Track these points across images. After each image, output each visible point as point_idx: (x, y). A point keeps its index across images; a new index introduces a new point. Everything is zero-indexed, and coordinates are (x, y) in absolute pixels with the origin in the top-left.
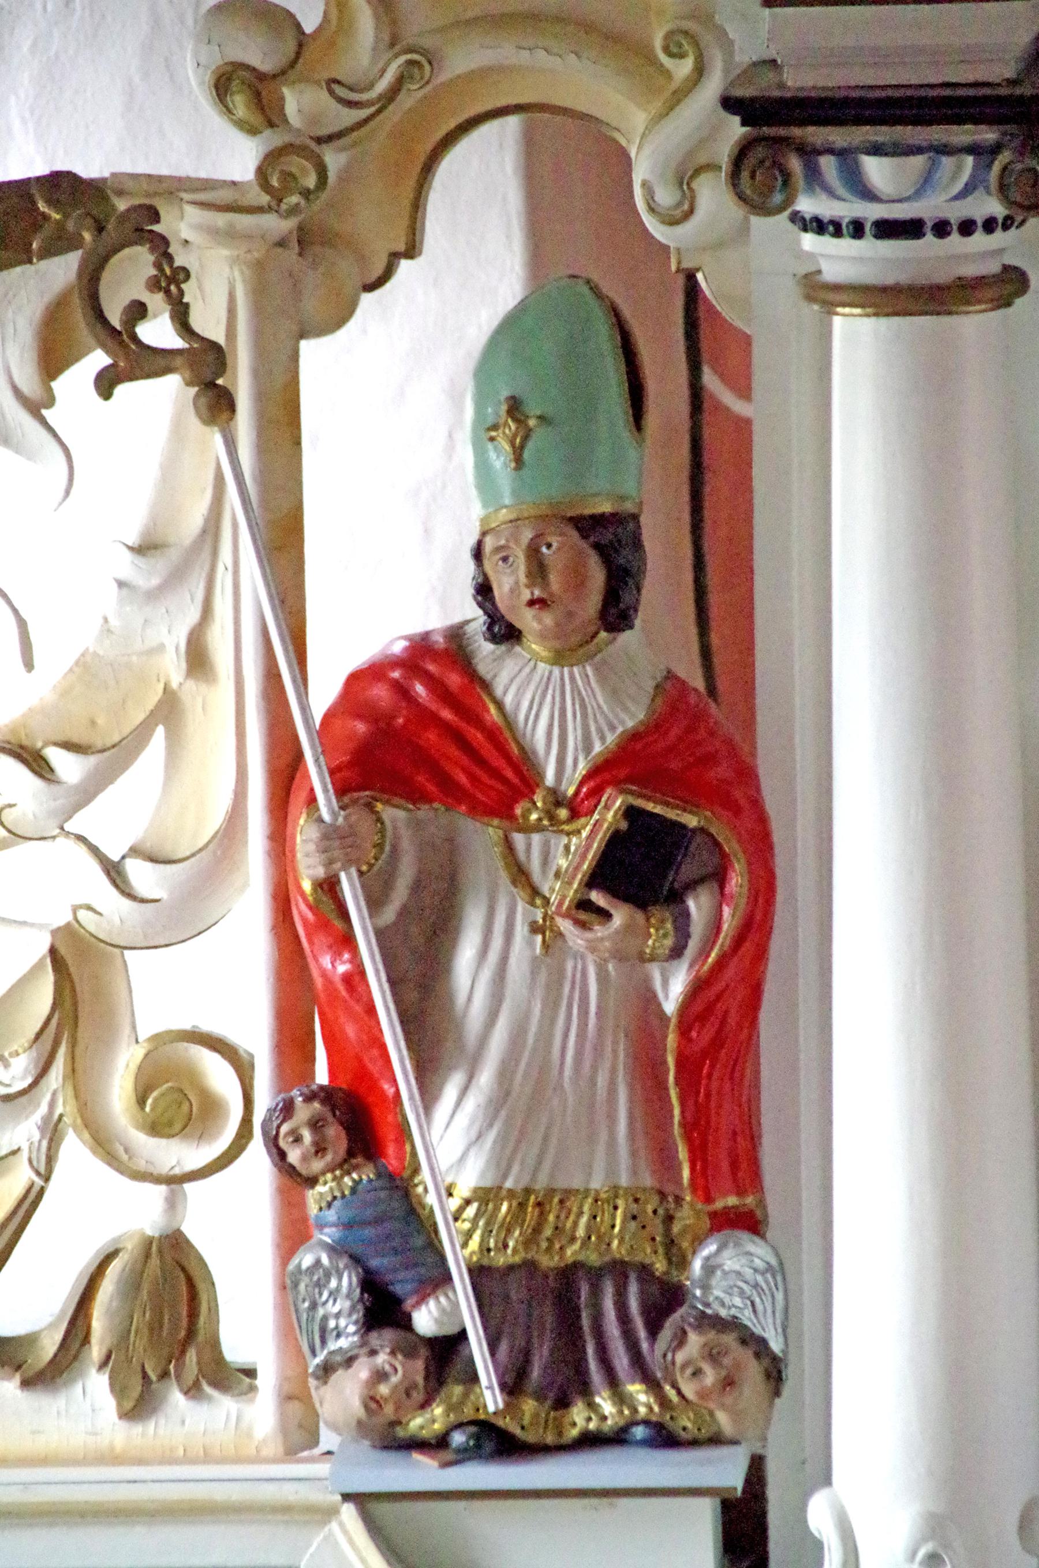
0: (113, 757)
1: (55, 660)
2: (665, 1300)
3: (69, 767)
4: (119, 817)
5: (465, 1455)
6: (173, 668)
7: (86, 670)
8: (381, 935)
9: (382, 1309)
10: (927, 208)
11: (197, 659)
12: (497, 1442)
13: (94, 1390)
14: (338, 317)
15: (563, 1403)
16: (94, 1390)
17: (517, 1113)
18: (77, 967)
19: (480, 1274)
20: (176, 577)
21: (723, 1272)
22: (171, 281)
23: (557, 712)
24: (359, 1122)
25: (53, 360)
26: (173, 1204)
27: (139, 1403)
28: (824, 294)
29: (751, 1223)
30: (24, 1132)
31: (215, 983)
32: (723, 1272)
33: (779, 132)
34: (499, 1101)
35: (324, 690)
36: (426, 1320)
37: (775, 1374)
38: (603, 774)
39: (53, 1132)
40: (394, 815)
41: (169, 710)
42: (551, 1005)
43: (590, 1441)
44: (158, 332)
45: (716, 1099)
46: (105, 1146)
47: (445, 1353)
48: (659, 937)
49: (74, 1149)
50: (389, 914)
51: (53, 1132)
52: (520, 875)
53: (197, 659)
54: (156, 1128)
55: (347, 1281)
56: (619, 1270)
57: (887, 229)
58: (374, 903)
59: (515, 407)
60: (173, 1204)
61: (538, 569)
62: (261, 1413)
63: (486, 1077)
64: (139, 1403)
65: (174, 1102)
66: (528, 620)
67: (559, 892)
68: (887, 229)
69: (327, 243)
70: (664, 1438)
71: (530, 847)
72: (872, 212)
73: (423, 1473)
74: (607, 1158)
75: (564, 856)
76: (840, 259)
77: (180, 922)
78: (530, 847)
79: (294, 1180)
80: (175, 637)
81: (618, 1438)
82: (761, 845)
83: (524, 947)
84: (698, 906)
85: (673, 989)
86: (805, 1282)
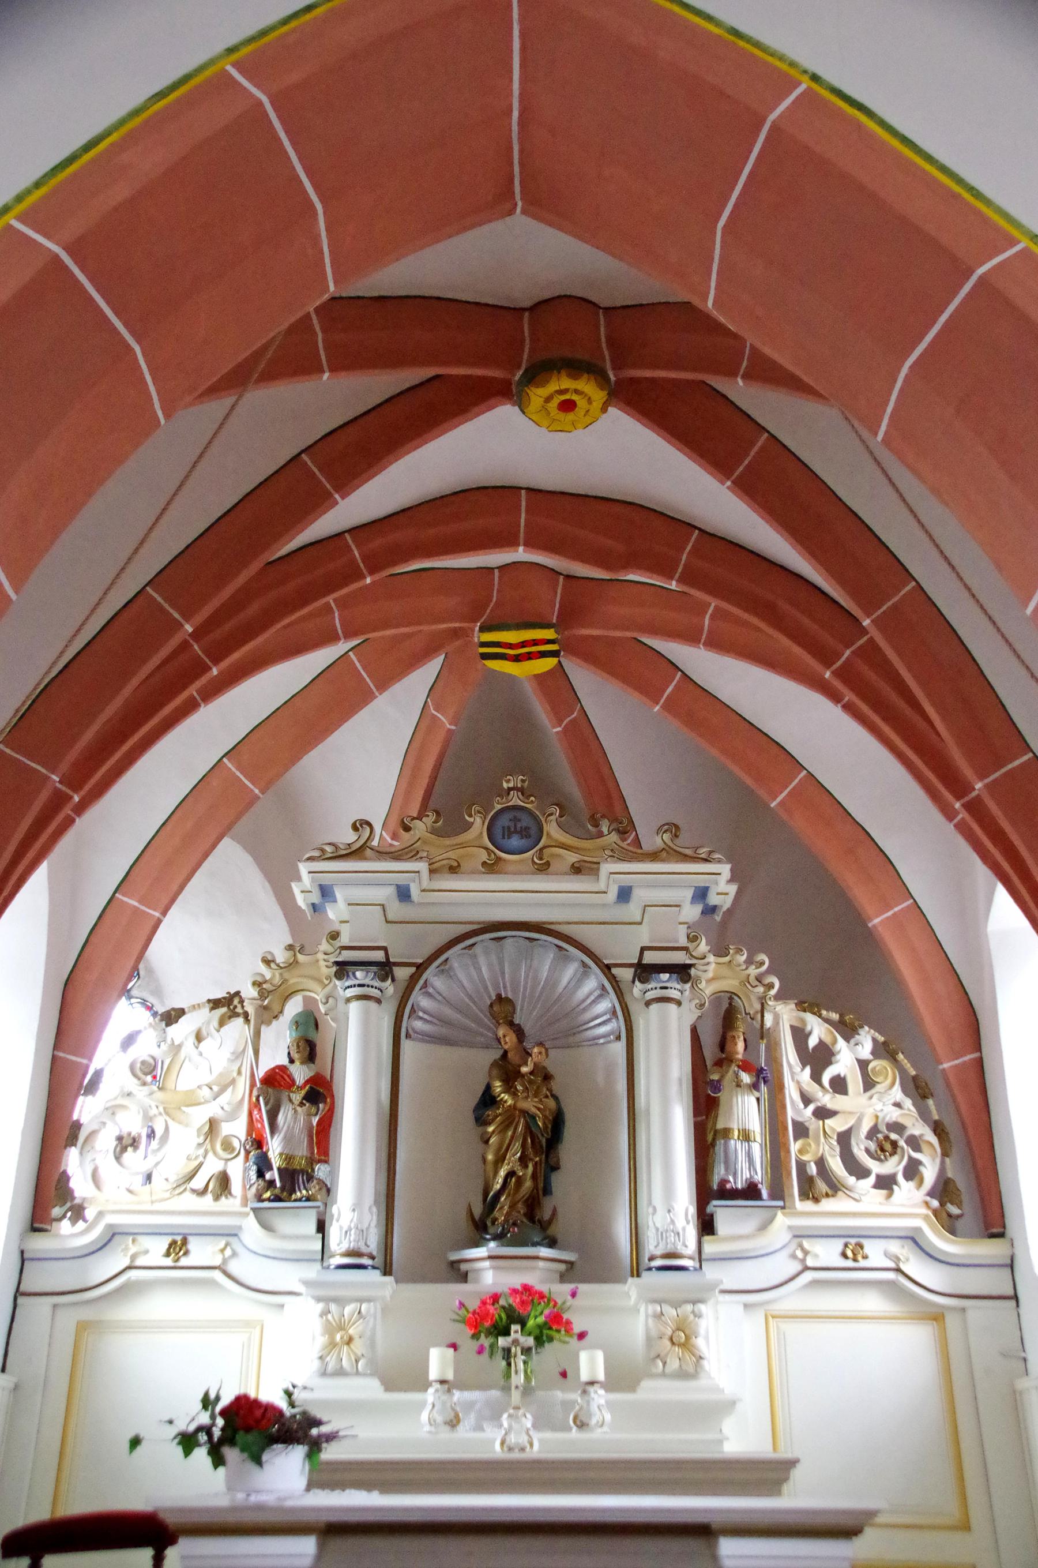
0: (223, 1090)
1: (216, 1072)
2: (310, 1178)
3: (216, 1088)
4: (225, 1098)
5: (273, 1201)
6: (235, 1074)
7: (221, 1074)
8: (268, 1112)
9: (260, 1174)
10: (367, 981)
11: (239, 1073)
12: (278, 1199)
13: (209, 1197)
14: (269, 1023)
15: (291, 1195)
16: (209, 1197)
17: (288, 1140)
18: (213, 1125)
19: (279, 1169)
20: (237, 1058)
21: (321, 1171)
22: (242, 1002)
23: (300, 1073)
24: (259, 1143)
25: (222, 1023)
26: (226, 1164)
27: (217, 1198)
28: (348, 1000)
29: (326, 1162)
30: (202, 1151)
31: (237, 1129)
32: (321, 1171)
33: (343, 969)
34: (285, 1137)
35: (261, 1073)
36: (268, 1176)
37: (328, 1191)
38: (307, 1082)
39: (206, 1152)
40: (270, 1090)
41: (233, 1082)
42: (295, 1123)
43: (295, 1200)
44: (239, 1010)
45: (322, 1139)
46: (215, 1153)
47: (271, 1183)
48: (314, 1110)
49: (210, 1154)
50: (269, 1107)
51: (206, 1152)
52: (291, 1100)
53: (239, 1073)
54: (224, 1150)
55: (255, 1168)
56: (303, 1171)
57: (360, 985)
58: (266, 1104)
59: (297, 1022)
60: (226, 1164)
61: (298, 1047)
62: (238, 1201)
63: (282, 1135)
64: (217, 1198)
65: (227, 1146)
66: (295, 1056)
67: (297, 1102)
68: (360, 985)
69: (268, 1014)
70: (308, 1199)
71: (293, 1096)
72: (357, 982)
73: (266, 1204)
74: (302, 1151)
75: (297, 1097)
76: (350, 993)
77: (232, 1116)
78: (293, 1096)
79: (248, 1153)
80: (236, 1069)
81: (300, 1200)
82: (333, 1097)
83: (291, 1113)
84: (321, 1106)
85: (315, 1121)
86: (334, 1174)
